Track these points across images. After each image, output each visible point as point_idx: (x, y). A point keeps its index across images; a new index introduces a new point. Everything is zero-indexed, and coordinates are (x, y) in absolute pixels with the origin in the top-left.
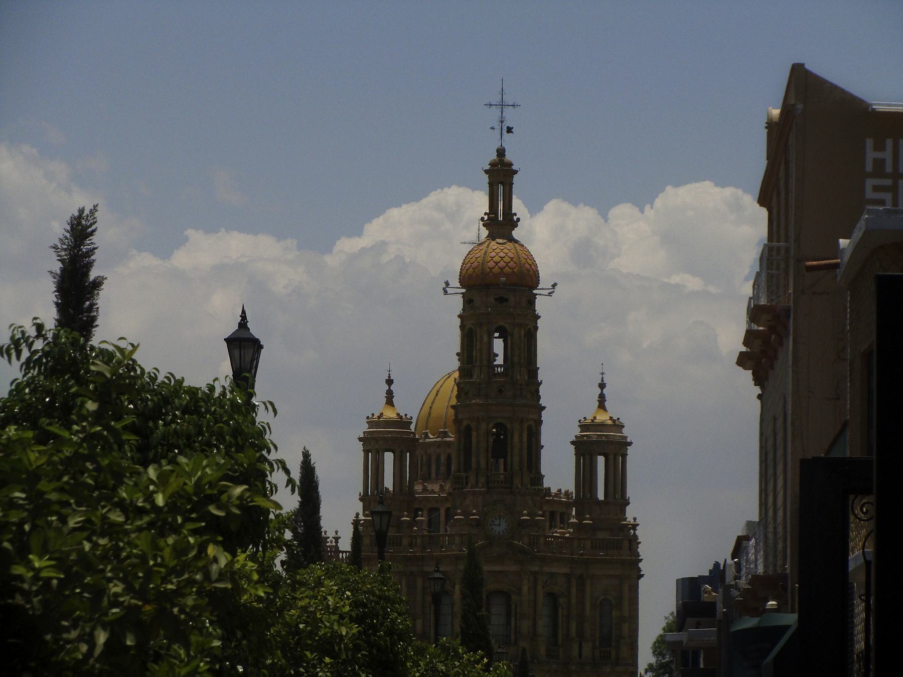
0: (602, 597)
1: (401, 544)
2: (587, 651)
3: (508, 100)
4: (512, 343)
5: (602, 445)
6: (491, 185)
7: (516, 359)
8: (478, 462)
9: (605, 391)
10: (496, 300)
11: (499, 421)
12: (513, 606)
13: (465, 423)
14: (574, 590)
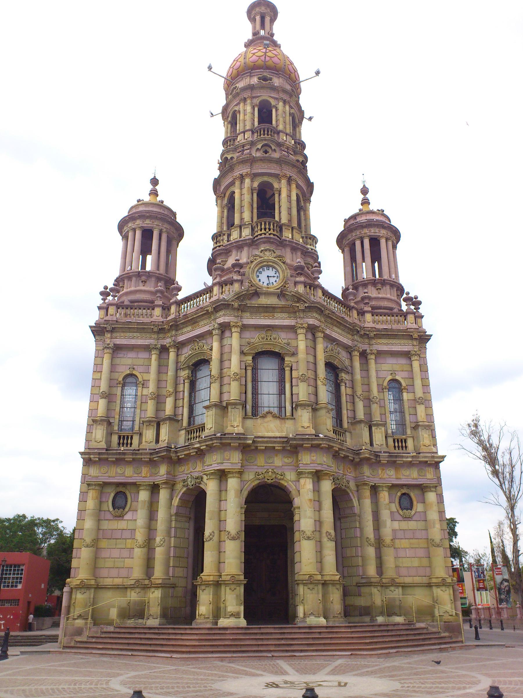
0: (390, 377)
5: (370, 237)
8: (242, 219)
9: (367, 196)
11: (266, 179)
12: (287, 369)
14: (357, 364)
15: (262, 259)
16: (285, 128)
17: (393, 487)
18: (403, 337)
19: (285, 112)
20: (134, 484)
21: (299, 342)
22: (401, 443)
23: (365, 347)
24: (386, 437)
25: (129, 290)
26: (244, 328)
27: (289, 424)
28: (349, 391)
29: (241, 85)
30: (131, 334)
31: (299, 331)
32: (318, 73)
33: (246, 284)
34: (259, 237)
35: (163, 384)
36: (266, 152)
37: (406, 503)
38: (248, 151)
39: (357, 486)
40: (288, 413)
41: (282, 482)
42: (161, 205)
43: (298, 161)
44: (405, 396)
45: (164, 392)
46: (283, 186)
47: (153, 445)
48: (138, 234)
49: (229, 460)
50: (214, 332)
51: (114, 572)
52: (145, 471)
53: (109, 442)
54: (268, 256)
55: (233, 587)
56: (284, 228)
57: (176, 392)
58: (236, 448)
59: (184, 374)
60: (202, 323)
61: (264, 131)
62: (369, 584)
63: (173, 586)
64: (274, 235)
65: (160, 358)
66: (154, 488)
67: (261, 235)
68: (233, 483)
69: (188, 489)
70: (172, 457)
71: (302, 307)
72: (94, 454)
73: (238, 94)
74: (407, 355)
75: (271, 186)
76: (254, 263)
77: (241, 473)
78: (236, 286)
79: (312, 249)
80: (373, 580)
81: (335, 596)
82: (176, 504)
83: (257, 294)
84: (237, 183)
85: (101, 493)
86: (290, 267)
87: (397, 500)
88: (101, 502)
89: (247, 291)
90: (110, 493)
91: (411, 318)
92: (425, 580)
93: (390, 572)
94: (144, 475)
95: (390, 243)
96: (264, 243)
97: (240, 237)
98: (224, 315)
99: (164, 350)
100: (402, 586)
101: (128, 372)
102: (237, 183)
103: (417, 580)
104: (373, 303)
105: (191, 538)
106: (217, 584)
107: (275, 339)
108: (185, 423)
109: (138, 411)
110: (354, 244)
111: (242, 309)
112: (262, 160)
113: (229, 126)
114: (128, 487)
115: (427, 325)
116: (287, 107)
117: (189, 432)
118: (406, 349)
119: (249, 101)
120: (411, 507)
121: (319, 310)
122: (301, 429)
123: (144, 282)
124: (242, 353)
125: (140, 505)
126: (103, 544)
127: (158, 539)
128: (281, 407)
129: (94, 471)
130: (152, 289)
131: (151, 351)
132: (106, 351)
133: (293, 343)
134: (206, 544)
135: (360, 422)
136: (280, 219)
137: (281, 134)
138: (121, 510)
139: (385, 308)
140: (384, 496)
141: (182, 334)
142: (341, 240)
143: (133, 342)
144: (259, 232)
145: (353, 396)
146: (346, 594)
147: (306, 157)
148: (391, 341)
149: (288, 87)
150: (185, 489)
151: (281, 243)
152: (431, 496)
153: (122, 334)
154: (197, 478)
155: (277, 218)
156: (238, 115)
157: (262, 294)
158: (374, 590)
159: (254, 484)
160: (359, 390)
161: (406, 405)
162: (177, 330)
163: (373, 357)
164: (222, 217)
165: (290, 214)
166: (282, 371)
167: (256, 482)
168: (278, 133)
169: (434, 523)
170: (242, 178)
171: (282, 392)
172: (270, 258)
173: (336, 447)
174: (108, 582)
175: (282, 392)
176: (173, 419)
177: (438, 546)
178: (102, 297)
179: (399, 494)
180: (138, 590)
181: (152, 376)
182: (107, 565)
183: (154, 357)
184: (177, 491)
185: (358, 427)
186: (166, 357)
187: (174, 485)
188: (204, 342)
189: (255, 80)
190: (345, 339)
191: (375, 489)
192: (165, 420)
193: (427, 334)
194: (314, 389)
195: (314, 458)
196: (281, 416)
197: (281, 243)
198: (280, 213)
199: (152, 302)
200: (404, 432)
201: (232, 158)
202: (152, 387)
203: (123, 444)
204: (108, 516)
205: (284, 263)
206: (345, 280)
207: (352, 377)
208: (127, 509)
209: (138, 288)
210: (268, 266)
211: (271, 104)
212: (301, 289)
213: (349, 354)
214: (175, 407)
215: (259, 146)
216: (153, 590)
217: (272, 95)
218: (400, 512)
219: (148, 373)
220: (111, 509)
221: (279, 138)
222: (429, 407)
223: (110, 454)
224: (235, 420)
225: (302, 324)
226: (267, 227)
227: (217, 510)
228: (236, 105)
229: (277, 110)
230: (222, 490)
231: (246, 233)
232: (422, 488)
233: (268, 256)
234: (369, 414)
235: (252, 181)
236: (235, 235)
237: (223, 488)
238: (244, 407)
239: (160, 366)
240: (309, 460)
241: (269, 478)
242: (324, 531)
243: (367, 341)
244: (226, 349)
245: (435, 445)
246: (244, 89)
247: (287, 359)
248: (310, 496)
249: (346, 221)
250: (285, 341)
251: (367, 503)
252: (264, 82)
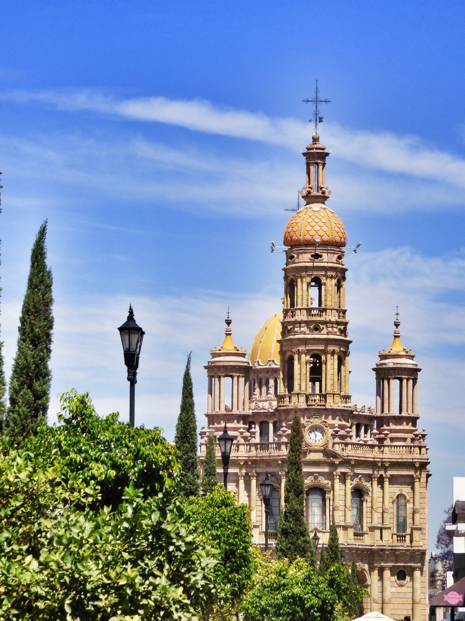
3: (322, 96)
6: (308, 165)
7: (329, 303)
10: (312, 256)
11: (316, 352)
13: (289, 354)
15: (312, 424)
23: (382, 472)
56: (327, 395)
64: (321, 405)
71: (337, 462)
79: (347, 407)
95: (411, 382)
140: (387, 573)
163: (387, 480)
166: (324, 500)
172: (318, 423)
179: (397, 571)
200: (405, 530)
213: (370, 478)
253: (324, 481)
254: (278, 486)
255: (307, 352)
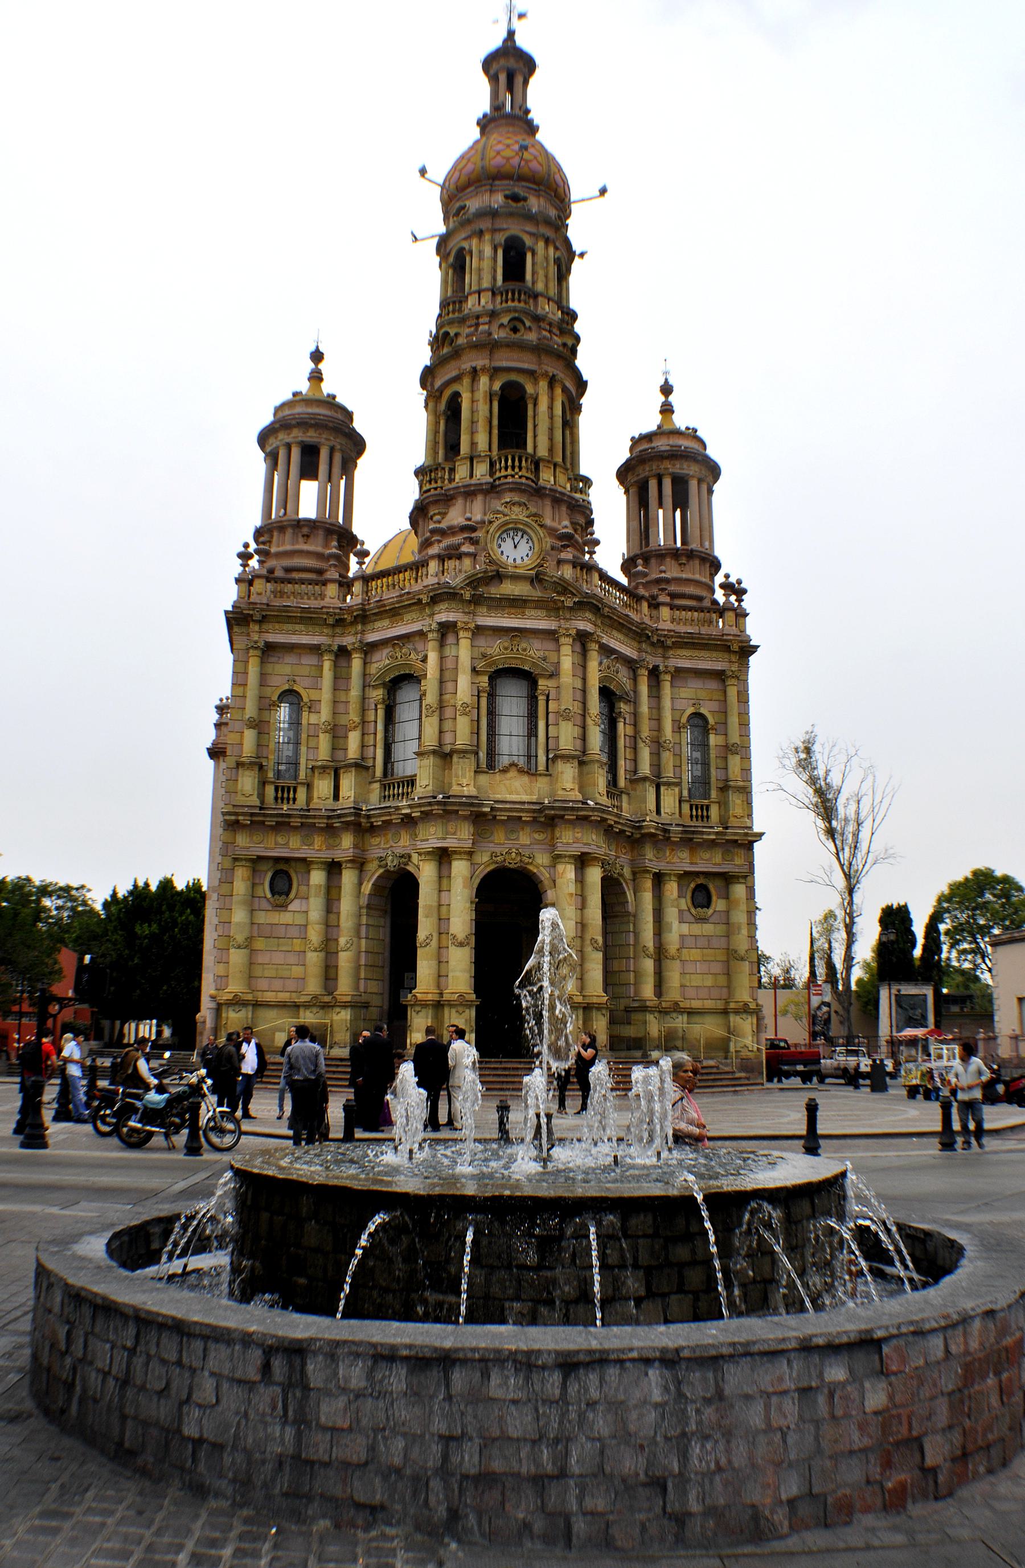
0: (691, 710)
1: (322, 596)
2: (669, 800)
4: (533, 264)
8: (473, 444)
9: (671, 398)
10: (506, 197)
11: (513, 377)
12: (542, 699)
14: (644, 689)
16: (546, 286)
17: (685, 877)
18: (715, 648)
19: (547, 259)
20: (303, 860)
21: (562, 658)
22: (701, 812)
23: (658, 661)
24: (680, 802)
25: (281, 549)
26: (479, 631)
27: (542, 783)
28: (630, 730)
29: (474, 204)
30: (290, 627)
31: (563, 640)
32: (603, 191)
33: (481, 558)
34: (503, 481)
35: (341, 708)
36: (515, 330)
37: (701, 897)
38: (486, 327)
39: (634, 873)
40: (541, 767)
41: (531, 867)
42: (330, 402)
43: (565, 345)
44: (713, 740)
45: (343, 720)
46: (541, 392)
47: (330, 803)
48: (296, 453)
49: (454, 834)
50: (430, 636)
51: (277, 984)
52: (318, 841)
53: (262, 796)
54: (518, 514)
55: (460, 1009)
57: (364, 722)
58: (465, 818)
59: (378, 694)
60: (407, 617)
61: (513, 294)
62: (644, 1009)
63: (366, 1006)
65: (336, 666)
66: (333, 868)
67: (506, 477)
68: (460, 868)
69: (387, 871)
70: (362, 825)
71: (569, 603)
72: (243, 814)
73: (469, 222)
74: (720, 676)
75: (520, 388)
76: (495, 525)
77: (470, 854)
78: (467, 562)
80: (648, 1004)
81: (600, 1025)
82: (367, 892)
83: (499, 576)
84: (466, 381)
85: (254, 871)
86: (552, 532)
87: (689, 895)
88: (254, 885)
89: (485, 572)
90: (266, 872)
91: (730, 616)
92: (720, 1005)
93: (673, 994)
94: (316, 848)
95: (704, 487)
96: (511, 490)
97: (471, 476)
98: (448, 610)
99: (343, 653)
100: (689, 1013)
101: (286, 687)
102: (466, 381)
103: (709, 1004)
104: (672, 588)
105: (388, 940)
106: (438, 1006)
107: (525, 650)
108: (379, 772)
109: (303, 749)
110: (647, 482)
111: (477, 601)
112: (510, 345)
113: (450, 272)
114: (293, 864)
115: (754, 629)
116: (551, 250)
117: (384, 787)
118: (718, 666)
119: (487, 237)
120: (708, 905)
121: (591, 605)
122: (560, 792)
123: (307, 536)
124: (474, 670)
125: (313, 891)
126: (260, 944)
127: (342, 941)
128: (530, 756)
129: (242, 840)
130: (319, 549)
131: (321, 655)
132: (252, 652)
133: (553, 657)
134: (419, 951)
135: (645, 779)
136: (535, 447)
137: (540, 299)
138: (284, 897)
139: (691, 597)
140: (671, 888)
141: (373, 630)
142: (624, 474)
143: (294, 639)
144: (503, 473)
145: (635, 738)
146: (612, 1022)
147: (577, 339)
148: (696, 653)
149: (553, 213)
150: (381, 871)
151: (538, 492)
152: (739, 890)
153: (277, 626)
154: (402, 857)
155: (530, 449)
156: (468, 259)
157: (507, 577)
158: (650, 1018)
159: (489, 869)
160: (645, 732)
161: (713, 754)
162: (364, 624)
163: (668, 677)
164: (436, 432)
165: (551, 439)
167: (492, 867)
168: (535, 296)
169: (739, 928)
170: (474, 373)
171: (532, 732)
173: (611, 820)
174: (269, 997)
175: (532, 732)
176: (361, 766)
177: (742, 959)
178: (240, 561)
179: (693, 885)
180: (315, 1010)
181: (326, 694)
182: (267, 974)
183: (327, 665)
184: (369, 874)
185: (640, 787)
186: (345, 664)
187: (362, 864)
188: (411, 646)
189: (498, 200)
190: (628, 651)
191: (659, 879)
192: (348, 766)
193: (752, 643)
194: (580, 730)
195: (579, 835)
196: (529, 771)
197: (538, 492)
198: (535, 436)
199: (320, 572)
200: (706, 795)
201: (457, 335)
202: (325, 714)
203: (282, 799)
204: (265, 905)
205: (541, 526)
206: (628, 541)
207: (635, 709)
208: (292, 895)
209: (297, 547)
210: (516, 530)
211: (524, 243)
212: (568, 572)
214: (363, 746)
215: (505, 320)
216: (338, 1010)
217: (527, 229)
218: (693, 910)
219: (318, 688)
220: (269, 895)
221: (536, 305)
222: (746, 758)
223: (265, 815)
224: (464, 776)
225: (567, 629)
226: (517, 463)
227: (435, 904)
228: (465, 239)
229: (533, 255)
230: (443, 876)
231: (481, 470)
232: (727, 879)
233: (518, 514)
234: (657, 766)
235: (491, 379)
236: (462, 472)
237: (445, 873)
238: (477, 753)
239: (336, 678)
240: (571, 839)
241: (512, 861)
242: (588, 937)
243: (660, 651)
244: (449, 664)
245: (750, 815)
246: (481, 214)
247: (541, 682)
248: (572, 888)
249: (636, 442)
250: (540, 654)
251: (647, 897)
252: (514, 204)
253: (534, 651)
254: (419, 664)
255: (495, 372)
